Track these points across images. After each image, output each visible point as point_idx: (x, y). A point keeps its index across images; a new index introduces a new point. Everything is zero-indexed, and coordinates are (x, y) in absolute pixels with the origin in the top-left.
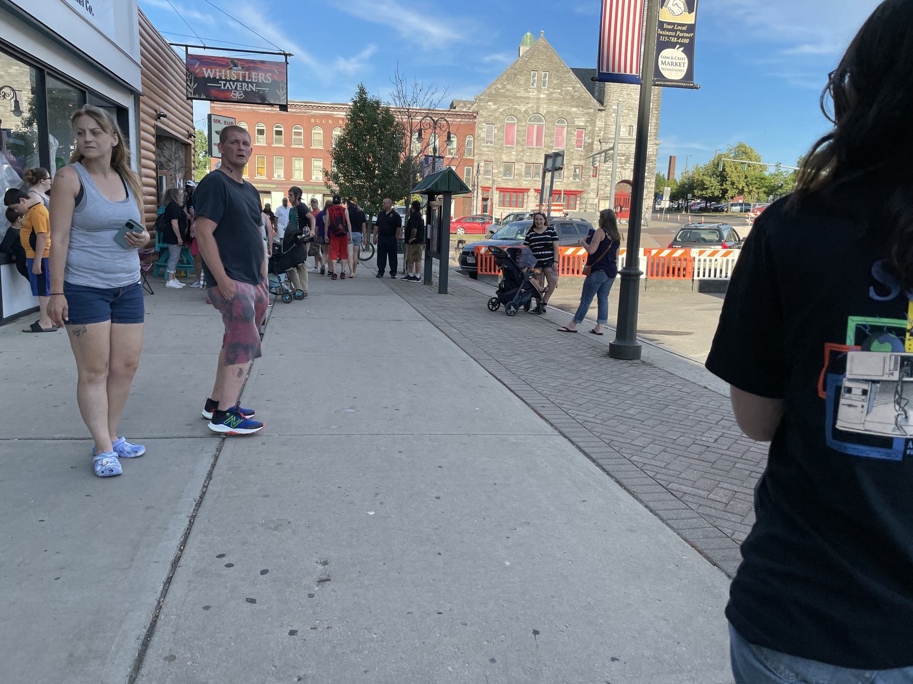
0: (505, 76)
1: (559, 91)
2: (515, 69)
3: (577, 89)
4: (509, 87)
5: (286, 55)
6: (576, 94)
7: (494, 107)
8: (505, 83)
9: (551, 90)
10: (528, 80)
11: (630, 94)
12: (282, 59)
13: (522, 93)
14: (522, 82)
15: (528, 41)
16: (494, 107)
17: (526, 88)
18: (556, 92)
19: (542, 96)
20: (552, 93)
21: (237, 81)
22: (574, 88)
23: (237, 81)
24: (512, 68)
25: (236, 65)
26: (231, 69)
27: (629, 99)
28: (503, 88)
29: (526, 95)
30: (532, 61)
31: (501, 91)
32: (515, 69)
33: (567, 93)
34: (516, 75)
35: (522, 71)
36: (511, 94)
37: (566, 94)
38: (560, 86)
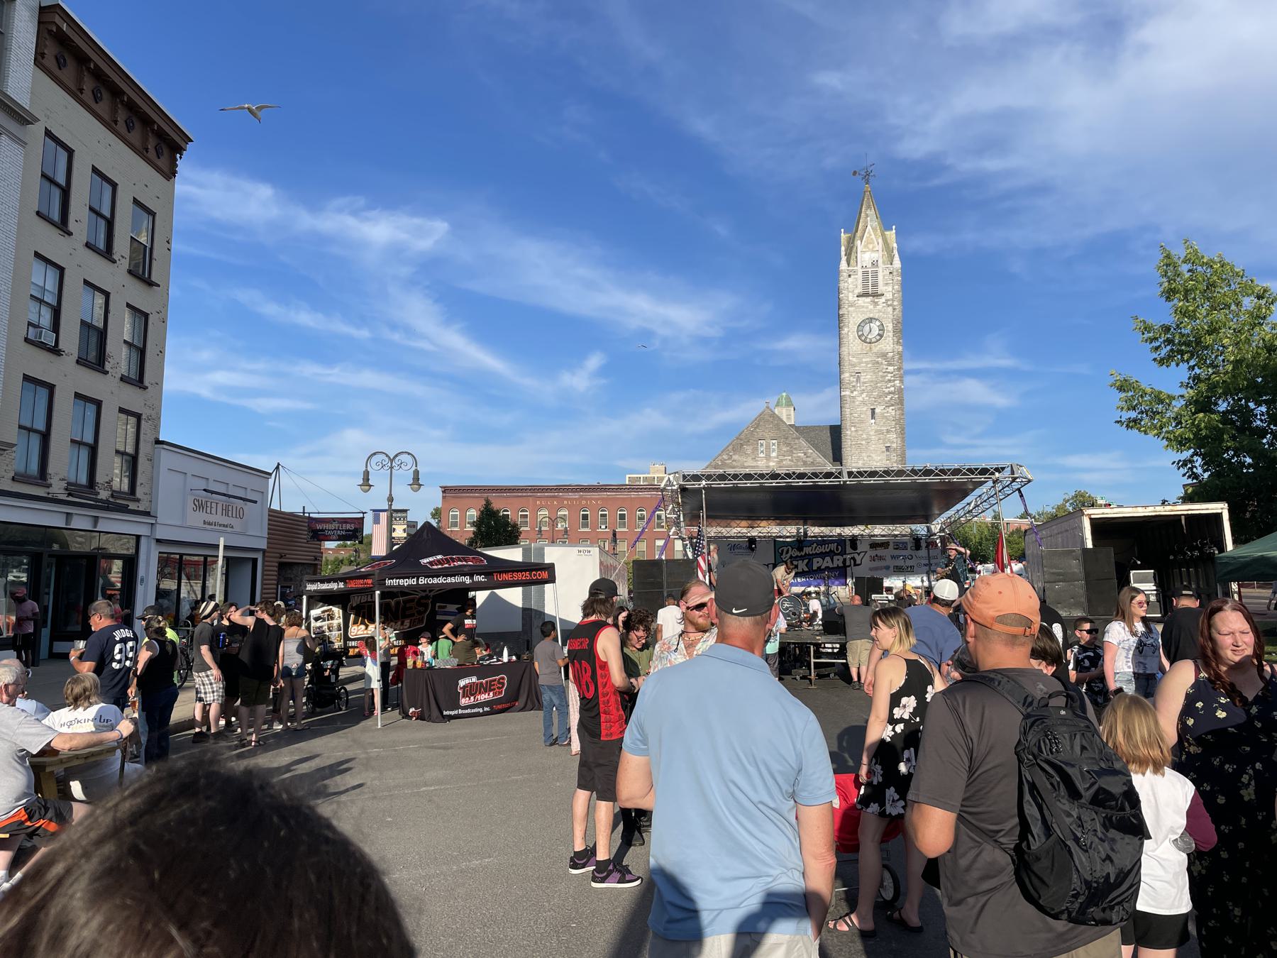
0: (731, 447)
1: (790, 458)
2: (741, 440)
3: (809, 455)
4: (735, 457)
5: (363, 513)
6: (808, 459)
8: (731, 454)
9: (781, 457)
11: (870, 456)
12: (361, 515)
15: (784, 401)
17: (753, 457)
18: (786, 459)
20: (782, 460)
21: (335, 530)
22: (805, 454)
23: (335, 530)
24: (737, 438)
25: (334, 521)
26: (332, 523)
27: (870, 461)
28: (729, 459)
29: (754, 464)
30: (758, 430)
31: (727, 462)
32: (741, 440)
33: (799, 459)
34: (742, 445)
35: (749, 441)
36: (739, 464)
37: (798, 461)
38: (791, 453)
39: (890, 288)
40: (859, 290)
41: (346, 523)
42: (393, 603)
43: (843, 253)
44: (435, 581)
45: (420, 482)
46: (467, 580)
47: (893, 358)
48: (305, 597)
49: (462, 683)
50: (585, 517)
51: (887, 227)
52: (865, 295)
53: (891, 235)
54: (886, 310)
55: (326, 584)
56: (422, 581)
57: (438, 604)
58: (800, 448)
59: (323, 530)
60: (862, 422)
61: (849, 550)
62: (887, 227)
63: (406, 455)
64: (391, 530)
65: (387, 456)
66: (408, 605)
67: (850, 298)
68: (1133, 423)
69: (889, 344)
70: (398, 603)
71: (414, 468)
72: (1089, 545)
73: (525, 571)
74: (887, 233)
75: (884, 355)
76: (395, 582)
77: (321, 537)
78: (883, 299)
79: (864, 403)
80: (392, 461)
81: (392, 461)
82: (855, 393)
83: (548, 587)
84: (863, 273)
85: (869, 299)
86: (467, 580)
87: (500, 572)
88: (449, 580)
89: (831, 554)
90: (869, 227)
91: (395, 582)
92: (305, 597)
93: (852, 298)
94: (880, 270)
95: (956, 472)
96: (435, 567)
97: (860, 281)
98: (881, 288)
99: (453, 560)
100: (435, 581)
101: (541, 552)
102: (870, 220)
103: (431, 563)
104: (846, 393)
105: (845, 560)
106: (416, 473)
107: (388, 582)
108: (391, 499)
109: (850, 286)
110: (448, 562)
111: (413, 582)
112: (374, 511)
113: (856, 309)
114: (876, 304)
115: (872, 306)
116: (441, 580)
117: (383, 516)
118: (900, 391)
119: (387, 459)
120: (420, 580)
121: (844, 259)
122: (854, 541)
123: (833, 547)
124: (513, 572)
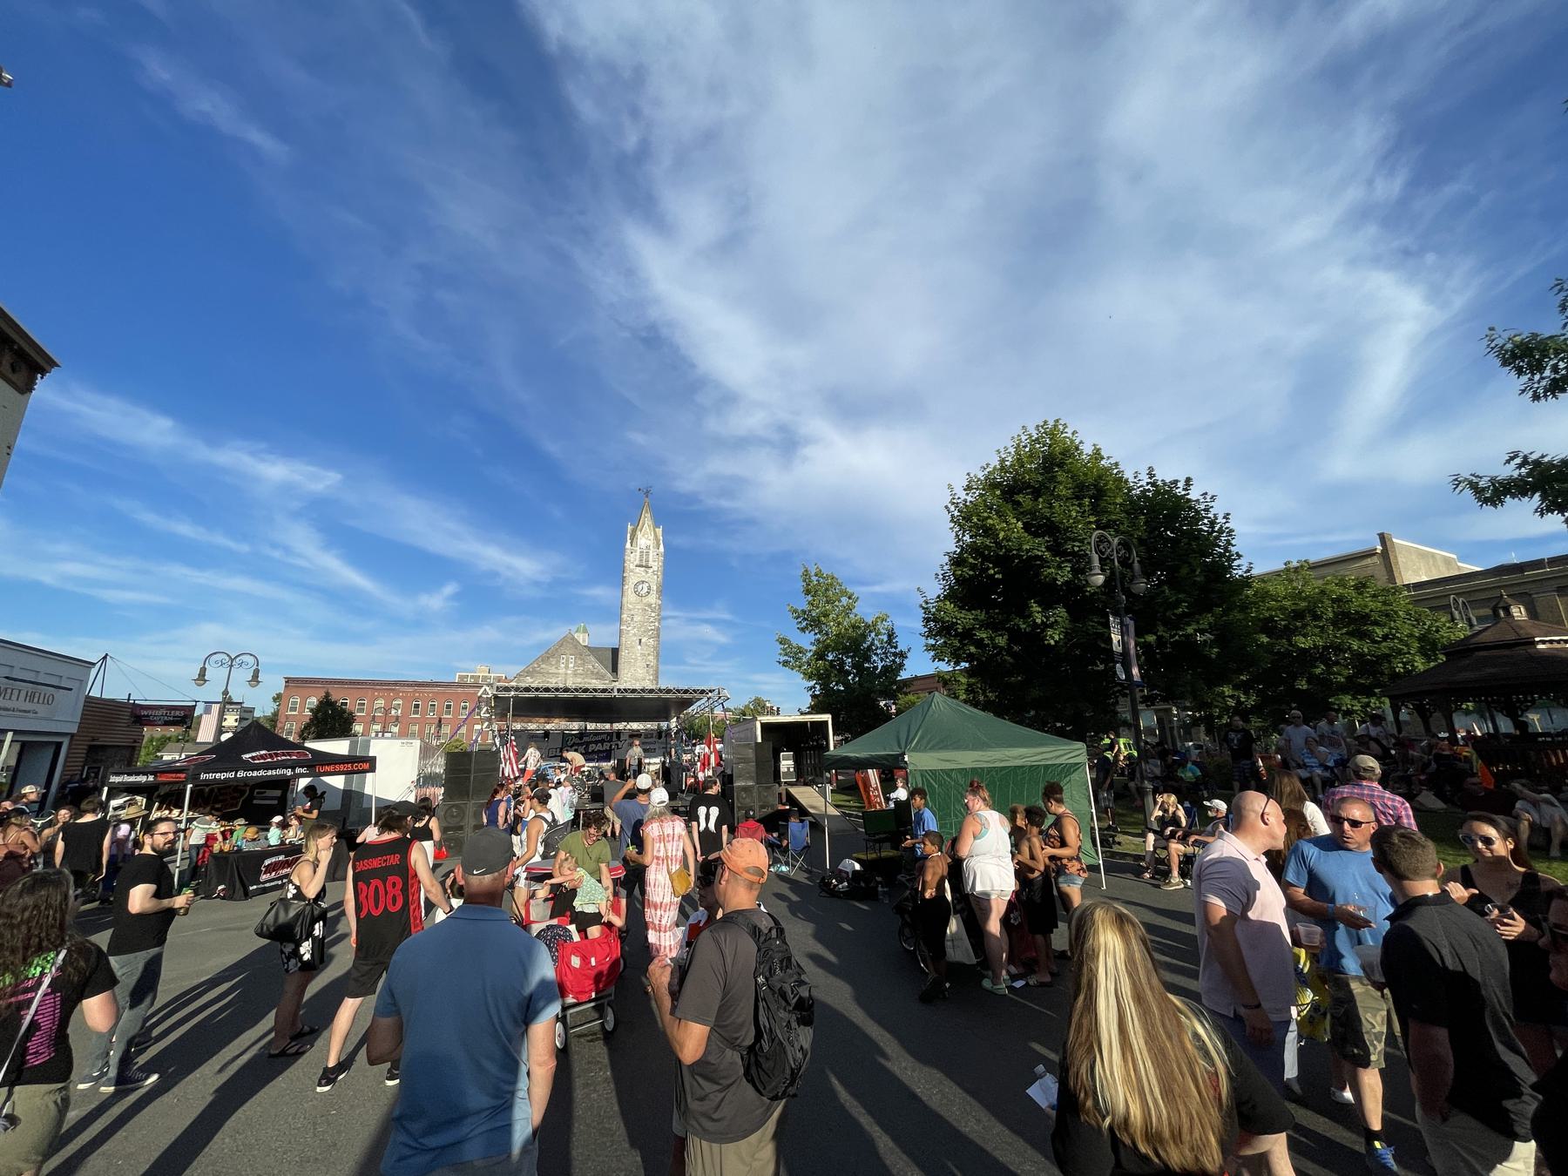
0: (540, 660)
4: (543, 666)
7: (532, 680)
10: (558, 662)
12: (194, 704)
13: (553, 670)
14: (553, 663)
16: (532, 680)
19: (569, 672)
29: (556, 671)
34: (548, 658)
39: (656, 564)
40: (637, 562)
41: (174, 709)
42: (207, 789)
43: (629, 538)
44: (255, 774)
45: (259, 679)
46: (289, 772)
47: (655, 608)
48: (106, 789)
49: (267, 862)
50: (417, 706)
51: (656, 525)
52: (639, 566)
53: (659, 531)
54: (653, 578)
55: (134, 777)
56: (241, 774)
57: (257, 791)
58: (590, 662)
59: (148, 716)
60: (632, 647)
61: (614, 738)
62: (656, 525)
63: (249, 656)
64: (221, 718)
65: (228, 655)
66: (222, 791)
67: (631, 567)
68: (785, 663)
69: (653, 599)
70: (212, 791)
71: (255, 667)
72: (759, 740)
73: (348, 763)
74: (657, 530)
75: (650, 606)
76: (211, 776)
77: (145, 722)
78: (650, 571)
79: (635, 635)
80: (232, 660)
81: (232, 660)
82: (630, 628)
83: (369, 775)
84: (641, 552)
85: (643, 569)
86: (289, 772)
87: (322, 765)
88: (269, 773)
89: (602, 741)
90: (646, 524)
91: (211, 776)
92: (106, 789)
93: (632, 566)
94: (651, 552)
95: (686, 691)
96: (258, 762)
97: (638, 557)
98: (650, 564)
99: (277, 755)
100: (255, 774)
101: (367, 746)
102: (647, 520)
103: (253, 758)
104: (624, 627)
105: (611, 746)
106: (256, 673)
107: (203, 776)
108: (226, 692)
109: (632, 559)
110: (271, 756)
111: (231, 775)
112: (206, 702)
113: (634, 575)
114: (647, 572)
115: (644, 574)
116: (262, 773)
117: (216, 708)
118: (658, 629)
119: (227, 659)
120: (239, 773)
121: (629, 541)
122: (619, 733)
123: (604, 737)
124: (336, 764)
